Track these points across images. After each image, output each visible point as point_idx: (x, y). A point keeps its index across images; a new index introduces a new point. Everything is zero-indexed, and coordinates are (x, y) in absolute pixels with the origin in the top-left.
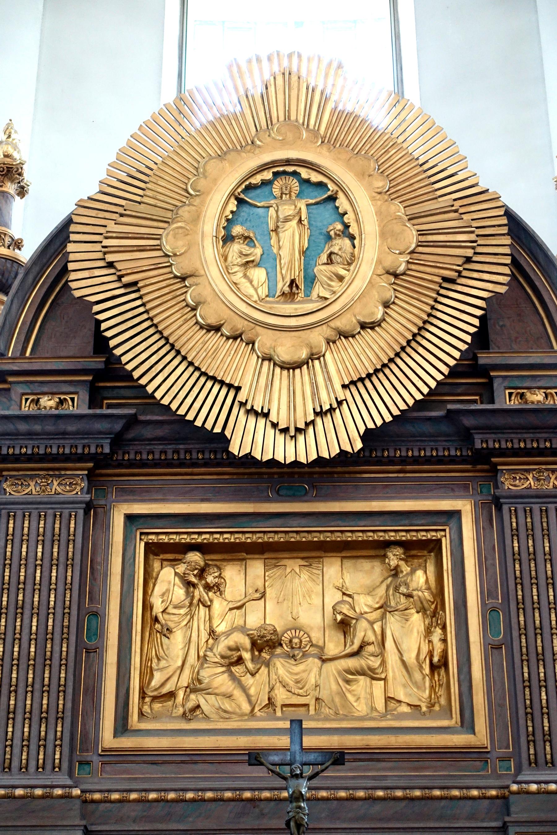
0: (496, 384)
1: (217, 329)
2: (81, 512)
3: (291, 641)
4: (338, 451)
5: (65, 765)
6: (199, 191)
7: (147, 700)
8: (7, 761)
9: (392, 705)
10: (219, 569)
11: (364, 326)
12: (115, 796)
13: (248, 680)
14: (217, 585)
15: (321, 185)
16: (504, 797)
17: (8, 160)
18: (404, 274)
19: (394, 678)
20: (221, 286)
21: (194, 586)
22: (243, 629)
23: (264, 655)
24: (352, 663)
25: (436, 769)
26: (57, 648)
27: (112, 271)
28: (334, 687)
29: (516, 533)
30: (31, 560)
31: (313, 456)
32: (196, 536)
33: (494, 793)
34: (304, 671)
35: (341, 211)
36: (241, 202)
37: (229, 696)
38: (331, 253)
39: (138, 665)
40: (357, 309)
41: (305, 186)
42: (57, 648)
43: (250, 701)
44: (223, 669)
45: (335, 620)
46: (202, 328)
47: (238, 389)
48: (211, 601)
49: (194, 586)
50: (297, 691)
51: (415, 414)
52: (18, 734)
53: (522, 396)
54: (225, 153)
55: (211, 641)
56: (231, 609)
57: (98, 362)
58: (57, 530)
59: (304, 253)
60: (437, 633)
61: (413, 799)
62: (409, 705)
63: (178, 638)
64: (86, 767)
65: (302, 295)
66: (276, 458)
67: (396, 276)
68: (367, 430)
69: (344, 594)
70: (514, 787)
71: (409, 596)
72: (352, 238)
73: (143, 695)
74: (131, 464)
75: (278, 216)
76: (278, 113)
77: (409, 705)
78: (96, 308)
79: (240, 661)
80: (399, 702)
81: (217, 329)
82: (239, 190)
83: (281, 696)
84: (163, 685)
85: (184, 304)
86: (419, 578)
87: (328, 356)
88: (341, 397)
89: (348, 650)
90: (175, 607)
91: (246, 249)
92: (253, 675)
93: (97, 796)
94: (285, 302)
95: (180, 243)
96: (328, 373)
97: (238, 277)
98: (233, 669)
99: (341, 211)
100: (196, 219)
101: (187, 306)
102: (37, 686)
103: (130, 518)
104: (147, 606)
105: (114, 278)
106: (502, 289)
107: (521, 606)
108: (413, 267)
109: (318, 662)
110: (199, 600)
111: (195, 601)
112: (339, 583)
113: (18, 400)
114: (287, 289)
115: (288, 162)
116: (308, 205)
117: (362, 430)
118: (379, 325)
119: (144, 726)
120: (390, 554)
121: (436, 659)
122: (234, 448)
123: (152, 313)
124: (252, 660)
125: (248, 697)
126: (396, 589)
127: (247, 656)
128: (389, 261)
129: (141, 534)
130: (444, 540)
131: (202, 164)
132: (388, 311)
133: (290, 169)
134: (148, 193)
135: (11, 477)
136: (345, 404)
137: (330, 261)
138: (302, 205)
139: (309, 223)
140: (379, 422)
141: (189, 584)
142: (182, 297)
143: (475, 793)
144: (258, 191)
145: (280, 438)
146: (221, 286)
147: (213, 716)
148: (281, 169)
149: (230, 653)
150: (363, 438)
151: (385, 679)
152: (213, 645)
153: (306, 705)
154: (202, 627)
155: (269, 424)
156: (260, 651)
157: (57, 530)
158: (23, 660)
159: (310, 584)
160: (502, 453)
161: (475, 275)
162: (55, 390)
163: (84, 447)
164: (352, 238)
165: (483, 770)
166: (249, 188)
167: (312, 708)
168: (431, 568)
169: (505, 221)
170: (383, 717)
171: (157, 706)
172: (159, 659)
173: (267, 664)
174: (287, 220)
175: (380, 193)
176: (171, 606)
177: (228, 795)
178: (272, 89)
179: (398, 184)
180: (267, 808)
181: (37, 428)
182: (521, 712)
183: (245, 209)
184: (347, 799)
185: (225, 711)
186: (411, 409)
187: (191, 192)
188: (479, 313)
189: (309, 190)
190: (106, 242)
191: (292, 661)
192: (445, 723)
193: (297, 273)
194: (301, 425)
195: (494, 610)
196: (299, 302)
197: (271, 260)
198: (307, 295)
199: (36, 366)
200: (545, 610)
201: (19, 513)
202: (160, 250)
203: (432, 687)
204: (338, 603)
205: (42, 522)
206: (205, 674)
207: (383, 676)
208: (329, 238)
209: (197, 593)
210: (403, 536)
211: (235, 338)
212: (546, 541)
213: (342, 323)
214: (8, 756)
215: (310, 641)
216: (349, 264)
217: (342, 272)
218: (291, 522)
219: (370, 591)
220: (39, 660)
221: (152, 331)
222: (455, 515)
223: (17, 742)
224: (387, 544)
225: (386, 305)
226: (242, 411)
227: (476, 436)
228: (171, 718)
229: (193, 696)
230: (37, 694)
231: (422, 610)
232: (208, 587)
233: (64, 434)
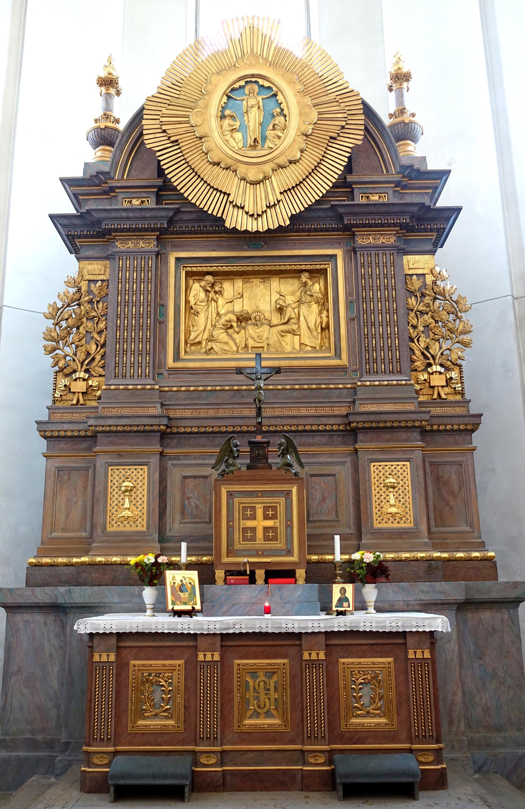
0: (355, 191)
1: (218, 164)
2: (154, 257)
3: (255, 318)
4: (278, 226)
5: (151, 375)
6: (208, 92)
7: (188, 345)
8: (124, 373)
9: (303, 346)
10: (221, 283)
11: (291, 162)
12: (175, 389)
13: (235, 336)
14: (220, 291)
15: (269, 88)
16: (354, 388)
17: (110, 76)
18: (311, 135)
19: (304, 334)
20: (220, 142)
21: (209, 292)
22: (233, 312)
23: (242, 324)
24: (284, 327)
25: (323, 376)
26: (145, 321)
27: (165, 134)
28: (276, 338)
29: (363, 265)
30: (131, 280)
31: (266, 228)
32: (209, 268)
33: (349, 386)
34: (262, 331)
35: (279, 102)
36: (229, 97)
37: (227, 343)
38: (275, 124)
39: (184, 329)
40: (287, 153)
41: (262, 88)
42: (145, 321)
43: (236, 346)
44: (224, 331)
45: (276, 307)
46: (210, 164)
47: (229, 195)
48: (217, 299)
49: (209, 292)
50: (258, 341)
51: (315, 207)
52: (129, 361)
53: (368, 197)
54: (221, 71)
55: (218, 318)
56: (227, 303)
57: (159, 182)
58: (143, 265)
59: (261, 124)
61: (312, 389)
62: (311, 346)
63: (202, 317)
64: (161, 376)
65: (260, 146)
66: (248, 229)
67: (307, 136)
68: (292, 215)
69: (280, 295)
70: (359, 383)
71: (311, 296)
72: (285, 116)
73: (186, 343)
74: (178, 233)
75: (247, 105)
76: (247, 49)
77: (311, 346)
78: (158, 154)
79: (231, 327)
80: (306, 345)
81: (218, 164)
82: (228, 91)
83: (251, 343)
84: (195, 338)
85: (201, 151)
86: (317, 287)
87: (273, 177)
88: (279, 199)
89: (283, 322)
90: (201, 302)
91: (232, 123)
92: (238, 333)
93: (166, 389)
94: (252, 150)
95: (199, 120)
96: (273, 186)
97: (228, 137)
98: (228, 331)
99: (279, 102)
100: (207, 107)
101: (203, 152)
102: (137, 339)
103: (178, 259)
104: (187, 302)
105: (166, 138)
106: (359, 143)
107: (364, 300)
108: (315, 131)
109: (268, 327)
110: (212, 299)
111: (210, 299)
112: (278, 290)
113: (121, 201)
114: (252, 143)
115: (253, 76)
116: (263, 99)
117: (290, 215)
118: (298, 162)
119: (187, 357)
120: (302, 276)
121: (324, 325)
122: (227, 225)
123: (186, 156)
124: (237, 326)
125: (236, 343)
126: (305, 293)
127: (235, 324)
128: (303, 128)
129: (183, 267)
130: (328, 269)
131: (209, 77)
132: (303, 154)
133: (254, 79)
134: (182, 93)
135: (120, 239)
136: (281, 202)
137: (274, 129)
138: (260, 98)
139: (263, 108)
140: (298, 211)
141: (207, 291)
142: (200, 148)
143: (341, 386)
144: (237, 92)
145: (250, 219)
146: (220, 142)
147: (219, 352)
148: (249, 79)
149: (226, 323)
150: (290, 219)
151: (300, 335)
152: (219, 320)
153: (263, 347)
154: (213, 311)
155: (244, 212)
156: (241, 322)
157: (143, 265)
158: (130, 327)
159: (264, 290)
160: (357, 226)
161: (346, 135)
162: (139, 196)
163: (154, 224)
164: (285, 116)
165: (345, 376)
166: (233, 90)
167: (265, 348)
168: (322, 283)
169: (362, 107)
170: (299, 352)
171: (193, 348)
172: (193, 326)
173: (244, 329)
174: (252, 107)
175: (299, 92)
176: (198, 302)
177: (227, 388)
178: (244, 36)
179: (308, 87)
180: (245, 393)
181: (131, 215)
182: (363, 349)
183: (231, 101)
184: (282, 389)
185: (225, 350)
186: (313, 204)
187: (204, 92)
188: (348, 155)
189: (264, 91)
190: (162, 119)
191: (256, 327)
192: (328, 355)
193: (258, 135)
194: (260, 213)
195: (351, 302)
196: (259, 150)
197: (245, 128)
198: (263, 146)
199: (129, 184)
200: (376, 302)
201: (124, 257)
202: (189, 123)
203: (322, 339)
204: (278, 299)
205: (136, 262)
206: (215, 333)
207: (299, 333)
208: (274, 116)
209: (210, 295)
210: (309, 267)
211: (227, 169)
212: (377, 269)
213: (280, 161)
214: (124, 371)
215: (265, 317)
216: (284, 130)
217: (280, 134)
218: (254, 260)
219: (293, 294)
220: (137, 327)
221: (186, 165)
222: (334, 257)
223: (128, 365)
224: (302, 271)
225: (302, 151)
226: (231, 206)
227: (345, 218)
228: (200, 353)
229: (210, 343)
230: (137, 343)
231: (317, 302)
232: (216, 292)
233: (144, 218)
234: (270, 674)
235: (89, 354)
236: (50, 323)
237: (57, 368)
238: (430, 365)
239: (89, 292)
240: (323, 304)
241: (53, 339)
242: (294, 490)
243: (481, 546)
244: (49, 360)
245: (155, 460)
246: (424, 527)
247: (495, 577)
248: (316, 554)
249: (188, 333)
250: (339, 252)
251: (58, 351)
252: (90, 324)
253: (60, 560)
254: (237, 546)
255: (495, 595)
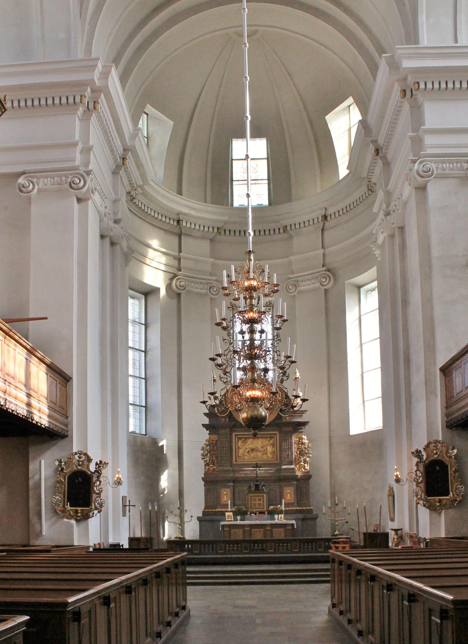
22: (250, 448)
60: (274, 449)
86: (271, 442)
103: (235, 435)
141: (243, 443)
222: (276, 434)
234: (260, 532)
235: (213, 460)
236: (202, 452)
237: (205, 463)
238: (300, 462)
239: (212, 444)
240: (273, 446)
241: (203, 456)
242: (265, 495)
243: (310, 506)
244: (203, 461)
245: (232, 488)
246: (296, 502)
247: (312, 513)
248: (288, 508)
249: (238, 454)
250: (277, 433)
251: (205, 459)
252: (213, 452)
253: (210, 510)
254: (252, 507)
255: (311, 517)
